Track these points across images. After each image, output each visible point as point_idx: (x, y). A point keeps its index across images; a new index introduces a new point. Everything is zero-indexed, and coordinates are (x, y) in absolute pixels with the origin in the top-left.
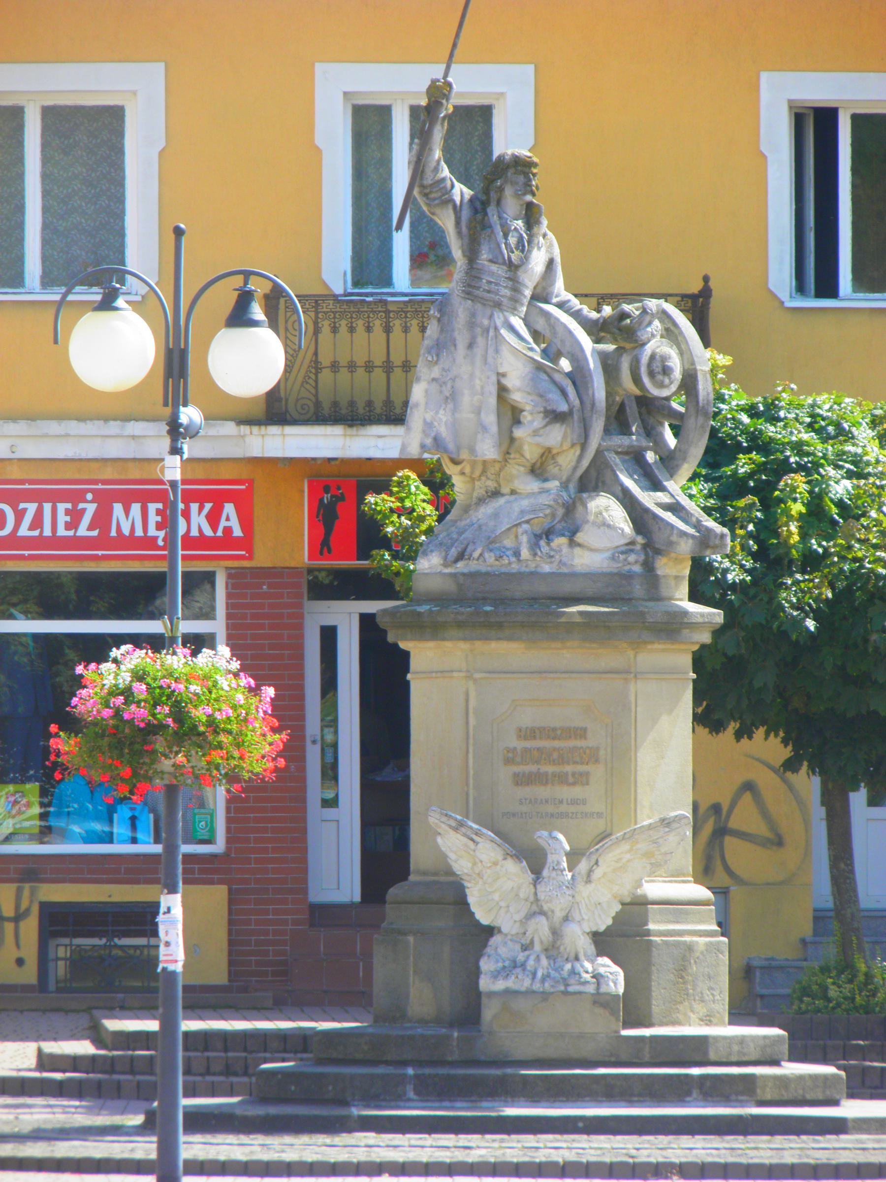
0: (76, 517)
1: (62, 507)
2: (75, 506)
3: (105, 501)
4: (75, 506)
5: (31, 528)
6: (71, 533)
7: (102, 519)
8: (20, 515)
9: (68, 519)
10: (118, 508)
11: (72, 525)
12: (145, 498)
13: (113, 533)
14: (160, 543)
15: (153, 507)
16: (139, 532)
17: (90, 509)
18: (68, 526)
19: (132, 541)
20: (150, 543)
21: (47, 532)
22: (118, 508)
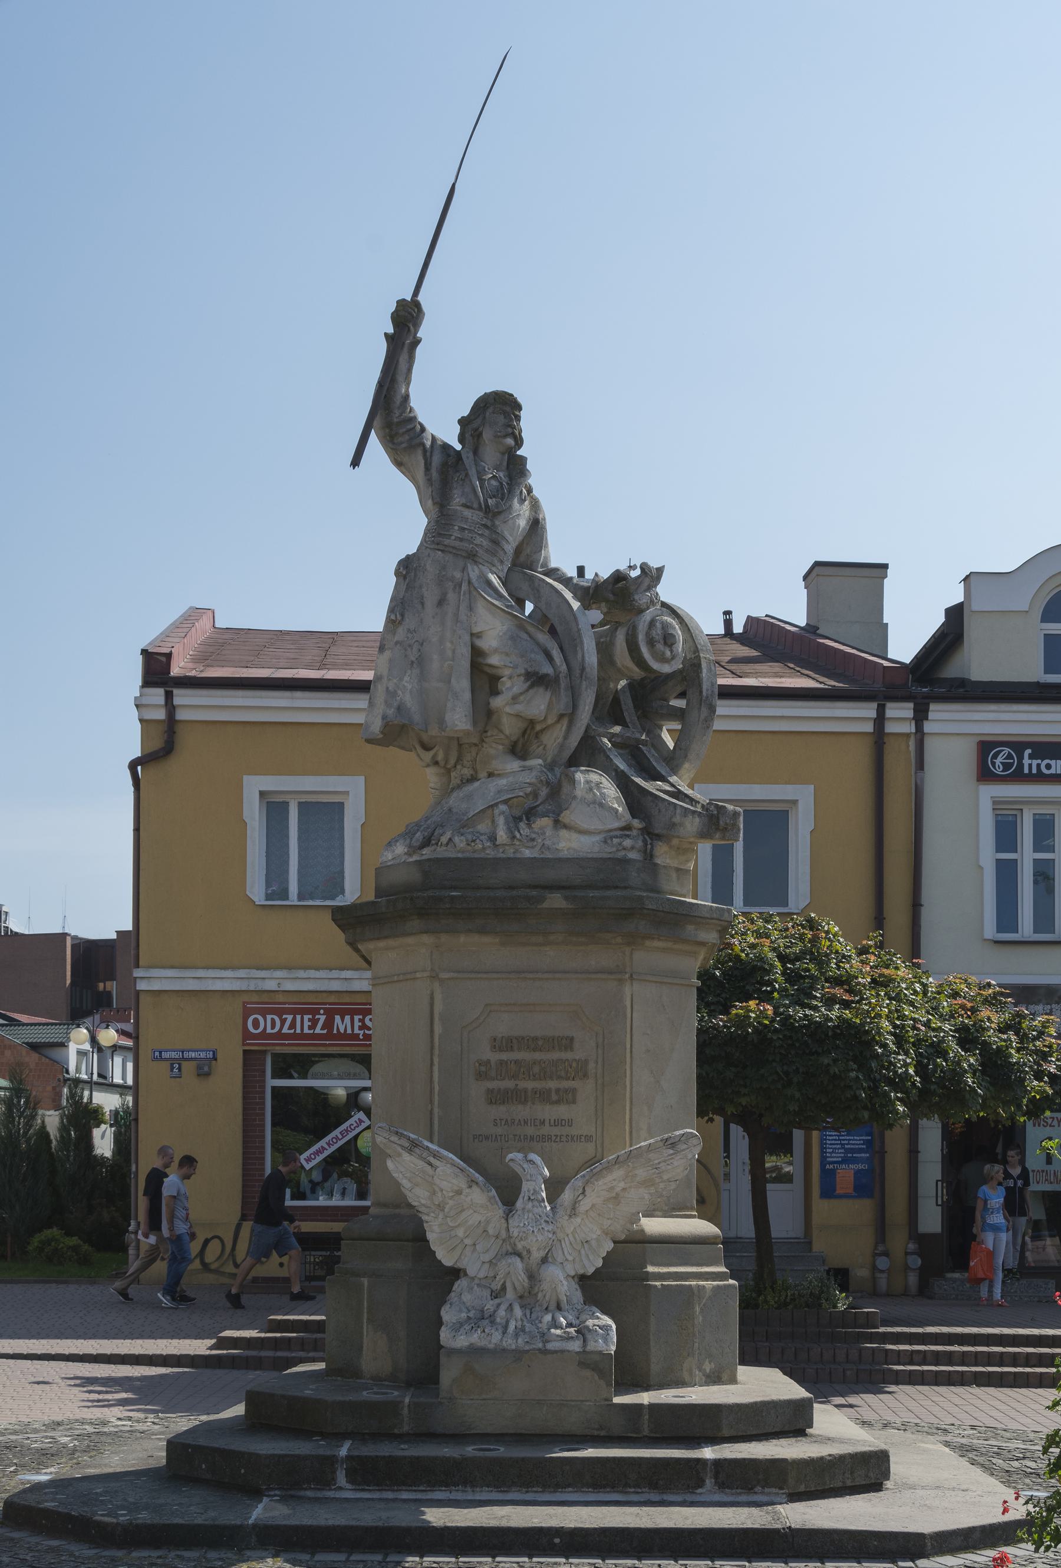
0: (314, 1023)
1: (306, 1017)
2: (314, 1016)
3: (330, 1014)
4: (314, 1016)
5: (289, 1029)
6: (312, 1032)
7: (329, 1024)
8: (283, 1022)
9: (310, 1024)
10: (338, 1018)
11: (313, 1027)
12: (352, 1013)
13: (335, 1032)
14: (361, 1037)
15: (356, 1018)
16: (349, 1031)
17: (323, 1018)
18: (310, 1028)
19: (344, 1036)
20: (355, 1037)
21: (298, 1031)
22: (338, 1018)
